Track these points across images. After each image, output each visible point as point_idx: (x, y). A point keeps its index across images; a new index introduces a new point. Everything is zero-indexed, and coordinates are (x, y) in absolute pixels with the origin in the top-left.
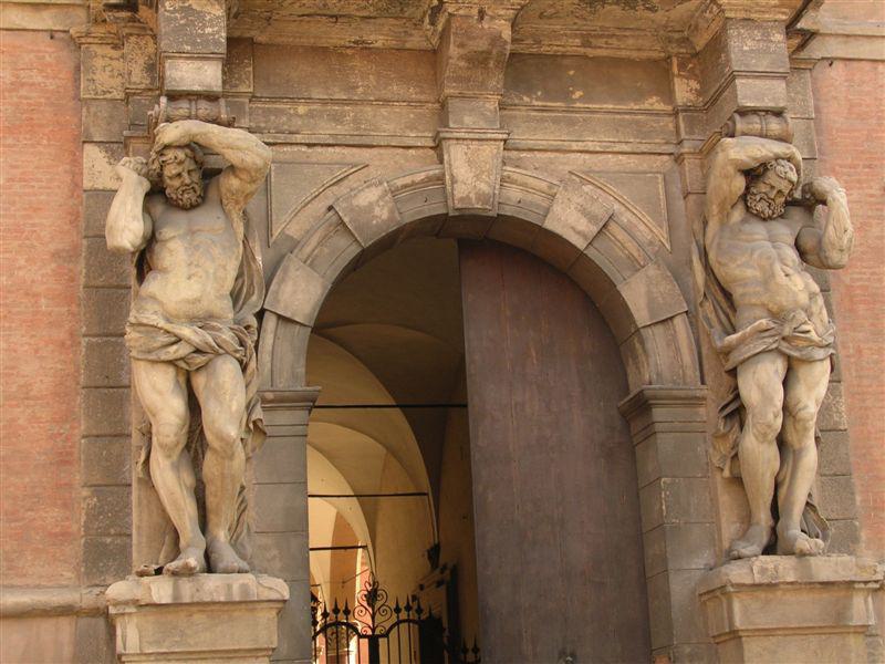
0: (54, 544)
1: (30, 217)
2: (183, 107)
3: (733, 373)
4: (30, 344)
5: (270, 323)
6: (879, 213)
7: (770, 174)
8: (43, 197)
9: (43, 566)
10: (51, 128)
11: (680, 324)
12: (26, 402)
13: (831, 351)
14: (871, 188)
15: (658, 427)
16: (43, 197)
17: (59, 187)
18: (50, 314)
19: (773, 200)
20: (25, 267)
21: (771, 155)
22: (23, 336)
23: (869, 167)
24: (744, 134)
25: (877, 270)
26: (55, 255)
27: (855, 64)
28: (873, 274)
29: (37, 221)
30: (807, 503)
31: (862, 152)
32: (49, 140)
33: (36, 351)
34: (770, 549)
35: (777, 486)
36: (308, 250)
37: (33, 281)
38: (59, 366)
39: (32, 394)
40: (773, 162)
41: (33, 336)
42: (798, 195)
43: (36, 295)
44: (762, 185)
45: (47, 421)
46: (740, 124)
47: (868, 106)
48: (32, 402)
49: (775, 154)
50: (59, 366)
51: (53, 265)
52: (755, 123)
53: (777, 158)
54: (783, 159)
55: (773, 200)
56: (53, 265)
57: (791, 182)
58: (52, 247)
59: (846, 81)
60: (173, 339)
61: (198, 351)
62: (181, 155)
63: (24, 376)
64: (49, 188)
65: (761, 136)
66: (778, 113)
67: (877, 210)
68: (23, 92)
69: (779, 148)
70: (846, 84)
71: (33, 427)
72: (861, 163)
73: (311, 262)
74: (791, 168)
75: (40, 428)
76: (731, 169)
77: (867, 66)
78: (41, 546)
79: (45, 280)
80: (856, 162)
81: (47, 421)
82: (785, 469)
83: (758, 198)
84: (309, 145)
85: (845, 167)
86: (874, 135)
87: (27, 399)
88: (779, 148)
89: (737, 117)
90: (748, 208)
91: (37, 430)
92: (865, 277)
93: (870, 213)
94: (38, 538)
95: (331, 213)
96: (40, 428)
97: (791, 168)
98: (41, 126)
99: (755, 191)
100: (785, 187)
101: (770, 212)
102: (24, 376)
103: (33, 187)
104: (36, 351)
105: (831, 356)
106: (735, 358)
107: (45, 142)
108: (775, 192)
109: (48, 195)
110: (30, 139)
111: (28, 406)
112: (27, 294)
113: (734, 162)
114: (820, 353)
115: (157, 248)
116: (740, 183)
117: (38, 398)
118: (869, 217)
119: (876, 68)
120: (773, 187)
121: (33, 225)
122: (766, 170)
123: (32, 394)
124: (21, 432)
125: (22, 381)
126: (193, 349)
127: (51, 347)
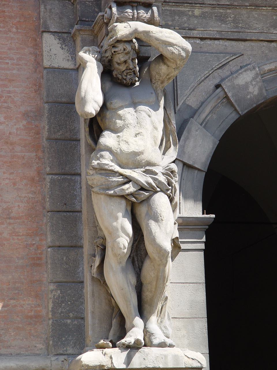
0: (30, 324)
1: (5, 86)
4: (10, 179)
8: (15, 72)
9: (22, 340)
10: (18, 19)
12: (8, 221)
16: (15, 72)
17: (26, 64)
18: (23, 158)
20: (4, 123)
22: (4, 173)
26: (26, 115)
29: (11, 89)
32: (17, 28)
33: (14, 184)
36: (203, 116)
37: (10, 133)
38: (31, 195)
39: (12, 215)
41: (12, 173)
43: (12, 144)
45: (23, 235)
48: (12, 221)
50: (31, 195)
51: (24, 122)
56: (24, 122)
58: (23, 109)
60: (126, 180)
61: (142, 189)
63: (5, 202)
64: (19, 65)
71: (13, 239)
73: (205, 125)
75: (18, 239)
78: (20, 325)
79: (19, 132)
81: (23, 235)
84: (202, 39)
87: (10, 218)
91: (16, 241)
94: (18, 319)
95: (219, 90)
96: (18, 239)
98: (10, 17)
102: (5, 202)
103: (8, 63)
104: (14, 184)
107: (14, 30)
109: (18, 70)
110: (4, 27)
111: (10, 224)
112: (7, 143)
115: (108, 114)
117: (17, 218)
121: (9, 92)
123: (12, 215)
124: (5, 242)
125: (5, 206)
126: (139, 188)
127: (25, 182)
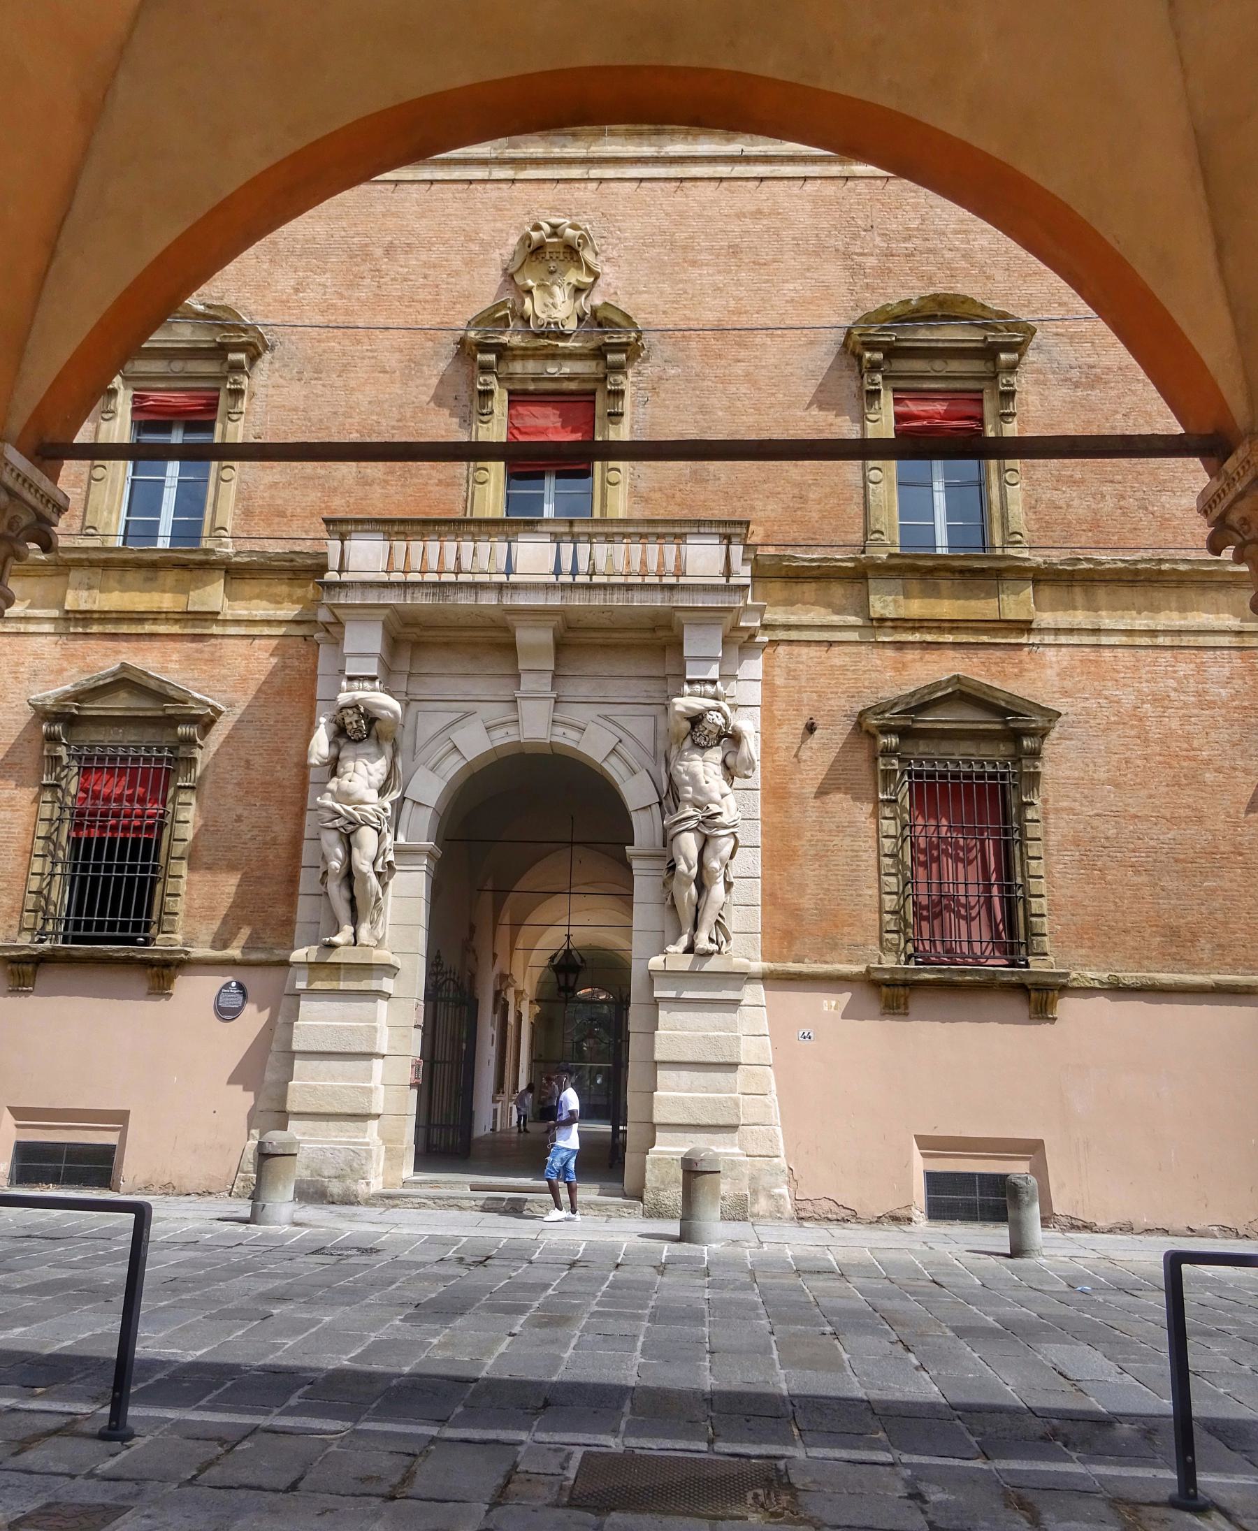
2: (356, 684)
5: (408, 804)
26: (297, 765)
52: (697, 688)
58: (295, 760)
61: (351, 823)
62: (350, 712)
68: (287, 671)
69: (711, 703)
76: (678, 718)
88: (711, 703)
89: (686, 687)
116: (687, 725)
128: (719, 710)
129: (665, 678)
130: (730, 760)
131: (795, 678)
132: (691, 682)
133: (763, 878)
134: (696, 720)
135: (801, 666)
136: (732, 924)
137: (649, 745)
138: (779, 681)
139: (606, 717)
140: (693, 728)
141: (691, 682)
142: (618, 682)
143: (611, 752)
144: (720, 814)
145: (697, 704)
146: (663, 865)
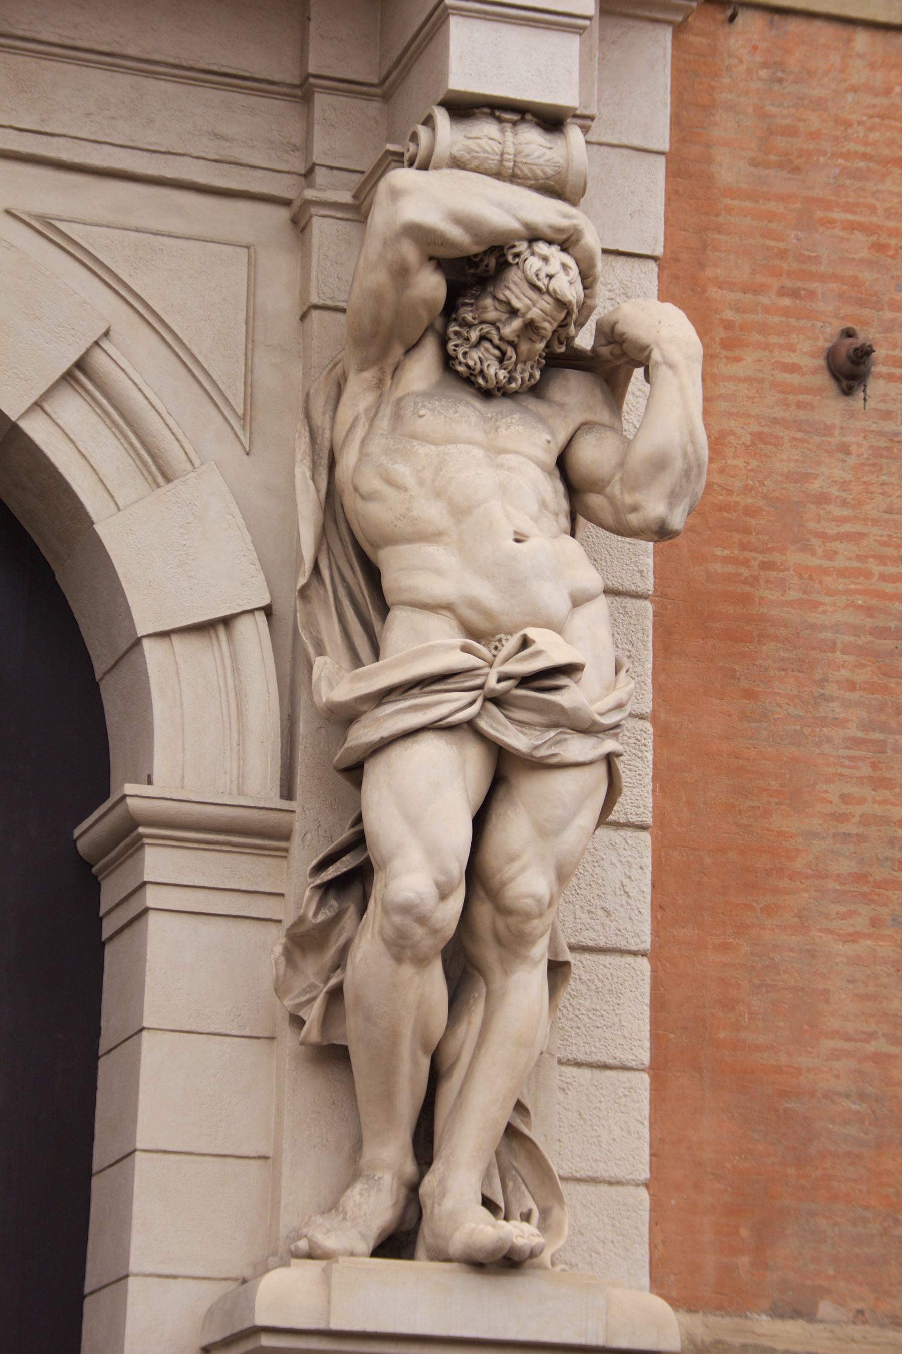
3: (354, 772)
6: (802, 415)
7: (514, 275)
11: (253, 634)
13: (610, 745)
14: (791, 348)
15: (152, 897)
19: (511, 343)
21: (515, 225)
23: (794, 294)
24: (456, 163)
25: (776, 557)
27: (794, 25)
28: (764, 566)
30: (511, 1132)
31: (782, 254)
34: (397, 1243)
35: (436, 1076)
40: (522, 246)
42: (585, 339)
44: (488, 302)
46: (448, 135)
47: (814, 136)
49: (527, 226)
52: (485, 135)
53: (534, 237)
54: (550, 242)
55: (511, 343)
57: (561, 304)
59: (765, 65)
65: (498, 175)
66: (551, 121)
67: (800, 405)
69: (546, 212)
70: (763, 73)
72: (776, 284)
74: (565, 266)
76: (410, 252)
77: (824, 32)
80: (760, 279)
82: (461, 1029)
83: (474, 335)
85: (731, 286)
86: (820, 214)
88: (546, 212)
89: (442, 117)
90: (447, 361)
92: (743, 570)
93: (779, 413)
97: (565, 266)
99: (469, 317)
100: (537, 309)
101: (502, 374)
105: (610, 759)
106: (365, 733)
108: (517, 323)
113: (418, 233)
114: (578, 748)
116: (431, 285)
118: (776, 421)
119: (849, 41)
120: (513, 312)
122: (503, 266)
128: (567, 241)
129: (302, 92)
130: (593, 455)
131: (791, 165)
132: (463, 108)
133: (655, 955)
134: (475, 269)
135: (814, 121)
136: (560, 1143)
137: (226, 369)
138: (729, 170)
139: (46, 228)
140: (450, 309)
141: (463, 108)
142: (117, 86)
143: (68, 377)
144: (570, 670)
145: (505, 207)
146: (292, 883)
